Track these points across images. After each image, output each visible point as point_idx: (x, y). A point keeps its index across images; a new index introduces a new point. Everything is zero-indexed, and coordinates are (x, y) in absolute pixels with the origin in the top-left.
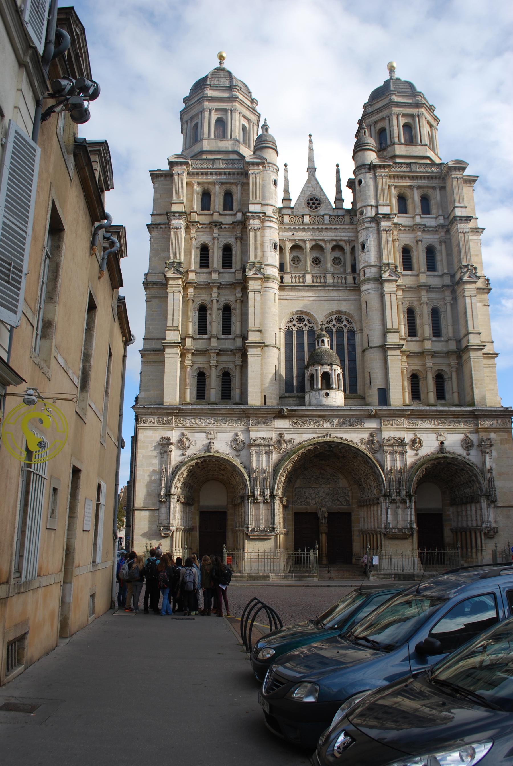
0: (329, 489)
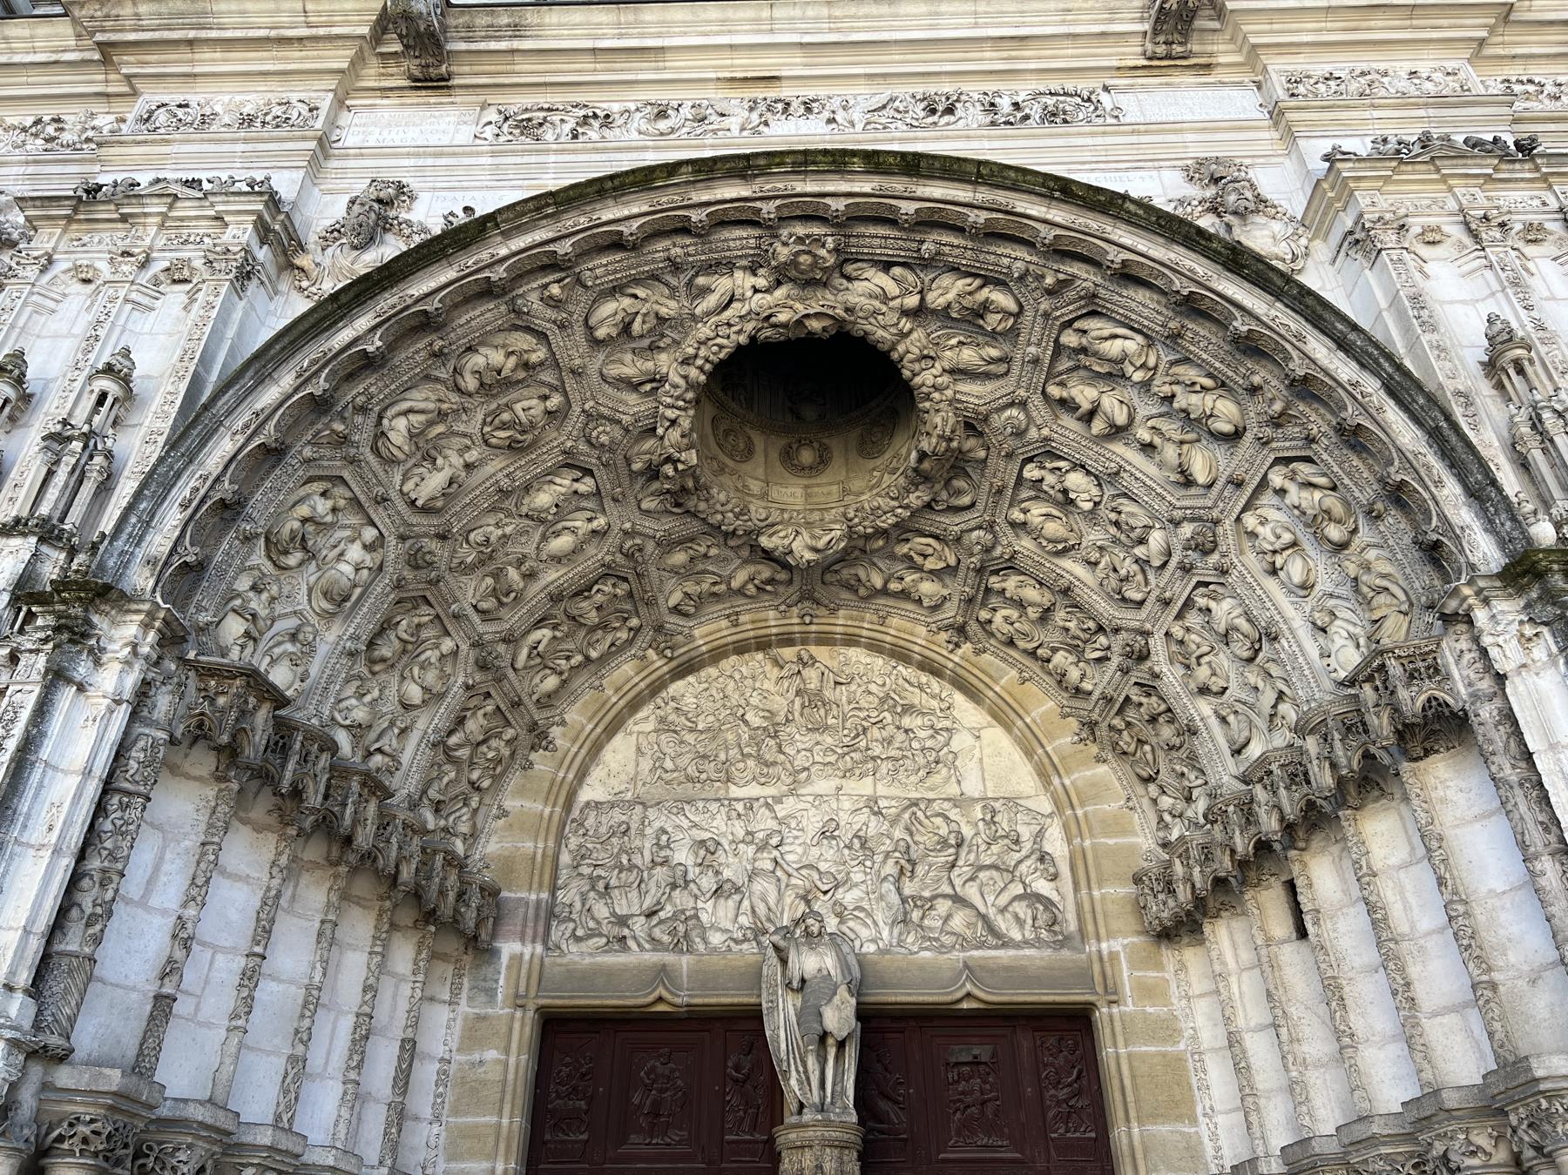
0: (872, 805)
